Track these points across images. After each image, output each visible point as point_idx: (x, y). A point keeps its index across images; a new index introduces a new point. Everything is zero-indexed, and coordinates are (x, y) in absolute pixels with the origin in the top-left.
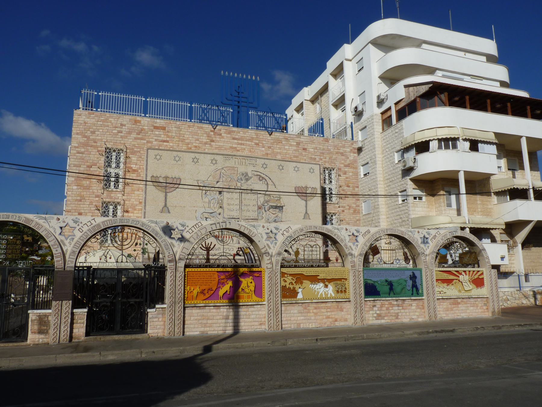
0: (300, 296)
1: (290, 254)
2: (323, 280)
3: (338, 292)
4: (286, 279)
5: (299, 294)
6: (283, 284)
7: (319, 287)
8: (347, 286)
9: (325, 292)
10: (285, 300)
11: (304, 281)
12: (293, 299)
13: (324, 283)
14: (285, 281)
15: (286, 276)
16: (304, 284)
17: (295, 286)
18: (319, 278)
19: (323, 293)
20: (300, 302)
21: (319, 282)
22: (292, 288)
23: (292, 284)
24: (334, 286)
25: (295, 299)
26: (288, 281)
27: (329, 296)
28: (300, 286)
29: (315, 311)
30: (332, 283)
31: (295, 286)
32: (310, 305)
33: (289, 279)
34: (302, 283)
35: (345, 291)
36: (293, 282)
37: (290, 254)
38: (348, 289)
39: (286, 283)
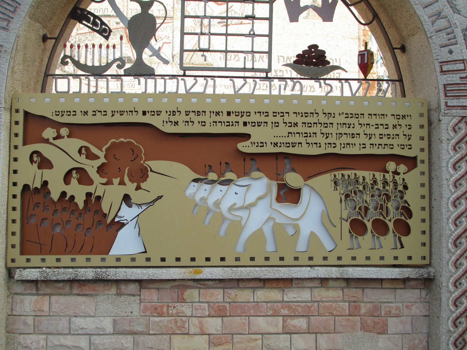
0: (126, 243)
1: (105, 32)
2: (273, 162)
3: (357, 227)
4: (46, 150)
5: (122, 234)
6: (31, 175)
7: (247, 202)
8: (413, 198)
9: (278, 229)
10: (36, 260)
11: (153, 164)
12: (81, 259)
13: (275, 175)
14: (45, 163)
15: (49, 133)
16: (153, 183)
17: (98, 186)
18: (244, 147)
19: (267, 230)
20: (122, 274)
21: (244, 173)
22: (80, 201)
23: (84, 178)
24: (336, 195)
25: (96, 259)
26: (62, 164)
27: (301, 246)
28: (130, 188)
29: (214, 325)
30: (325, 180)
31: (98, 186)
32: (193, 294)
33: (65, 153)
34: (140, 175)
35: (403, 228)
36: (91, 167)
37: (105, 32)
38: (417, 214)
39: (47, 174)
